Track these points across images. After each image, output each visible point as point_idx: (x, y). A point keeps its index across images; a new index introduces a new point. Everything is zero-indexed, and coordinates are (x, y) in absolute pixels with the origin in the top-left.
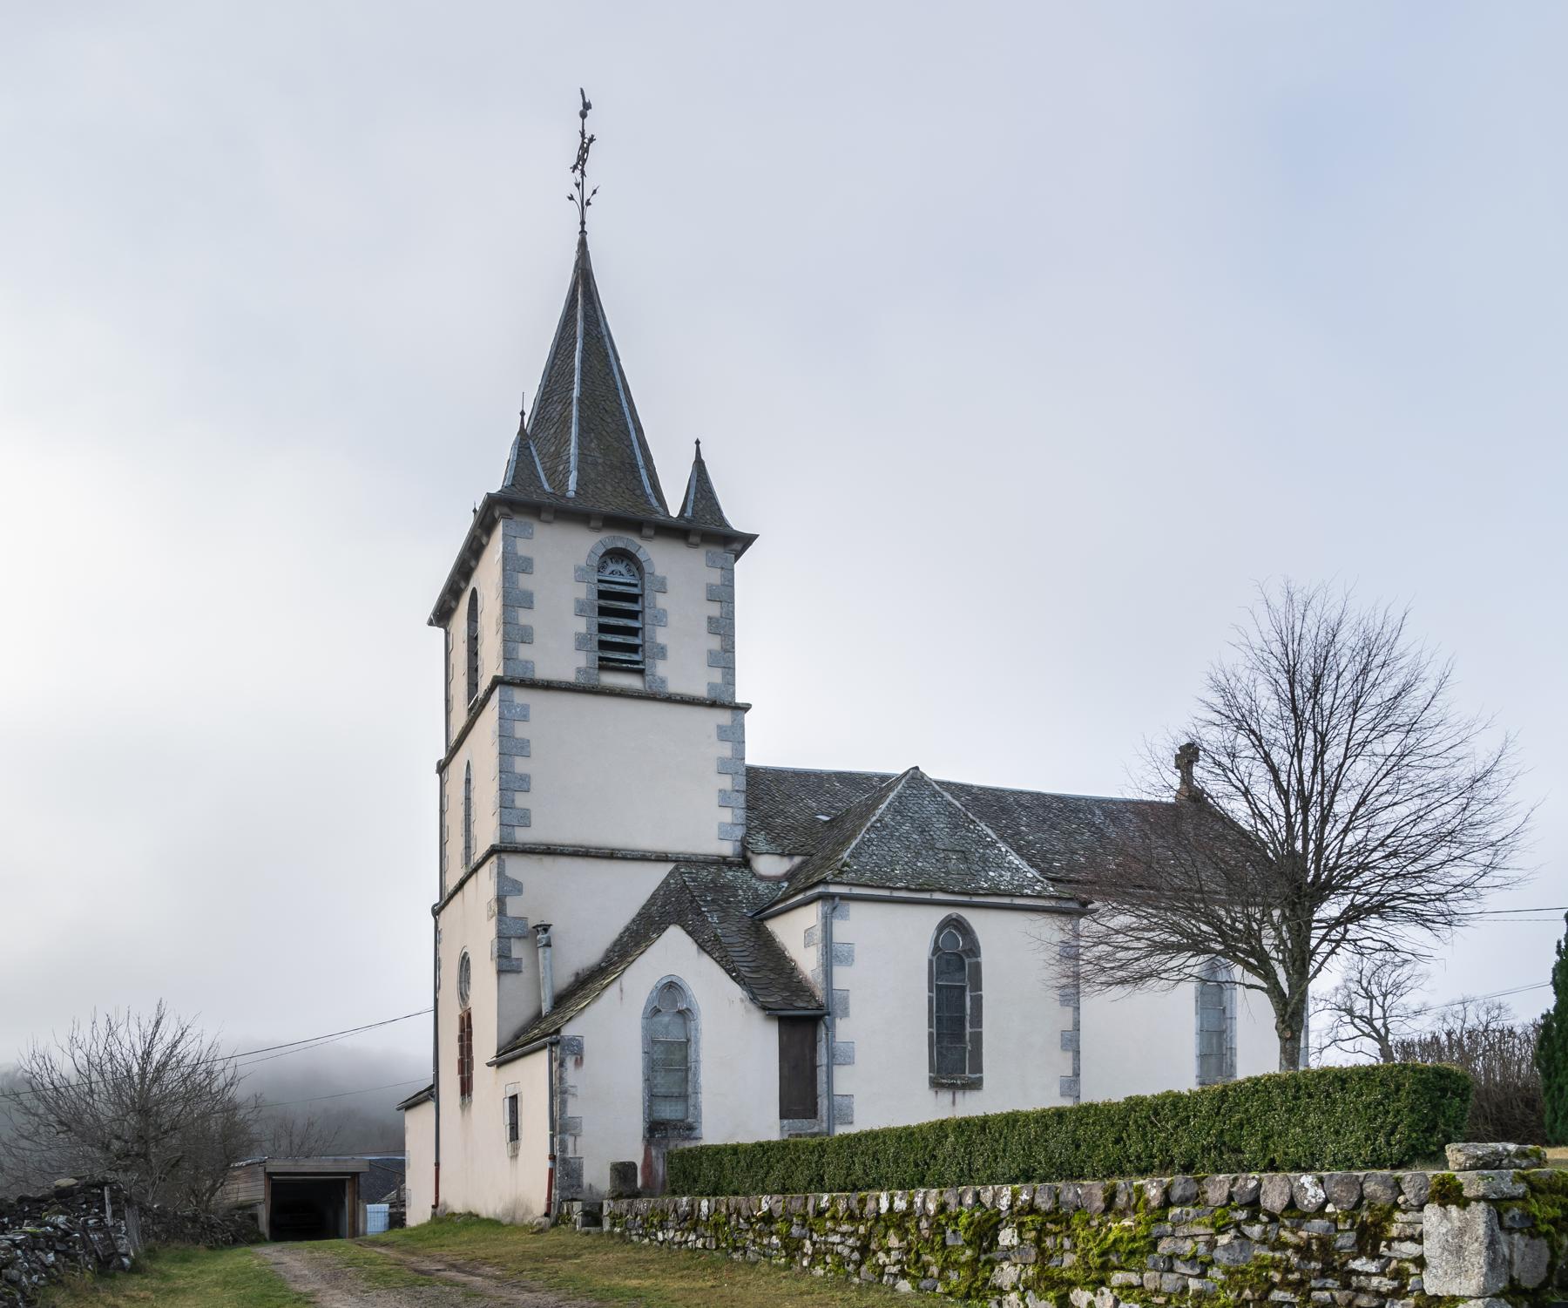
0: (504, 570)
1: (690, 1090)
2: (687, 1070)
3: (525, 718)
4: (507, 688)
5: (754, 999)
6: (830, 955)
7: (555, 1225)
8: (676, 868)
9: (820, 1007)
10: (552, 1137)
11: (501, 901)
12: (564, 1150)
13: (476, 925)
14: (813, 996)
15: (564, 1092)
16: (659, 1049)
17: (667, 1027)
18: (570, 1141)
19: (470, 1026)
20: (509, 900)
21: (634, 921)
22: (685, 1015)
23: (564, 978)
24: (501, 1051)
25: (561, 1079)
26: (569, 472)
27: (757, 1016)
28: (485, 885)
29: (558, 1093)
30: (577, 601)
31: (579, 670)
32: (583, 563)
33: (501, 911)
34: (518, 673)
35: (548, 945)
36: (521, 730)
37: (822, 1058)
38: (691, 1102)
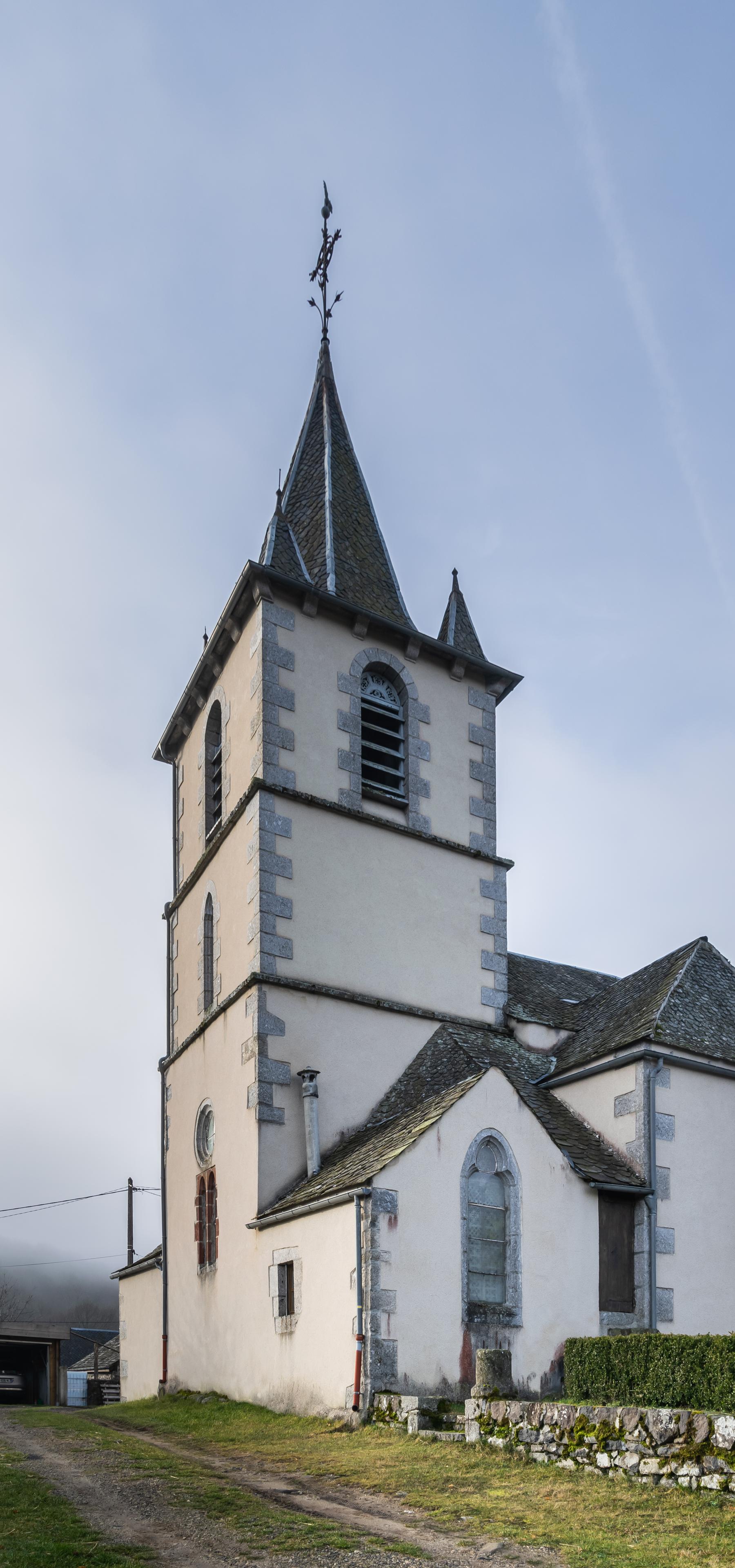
0: (264, 660)
1: (509, 1269)
2: (505, 1245)
3: (286, 834)
4: (268, 796)
5: (575, 1168)
6: (653, 1127)
7: (367, 1421)
8: (443, 1028)
9: (642, 1184)
10: (360, 1312)
11: (261, 1039)
12: (376, 1330)
13: (228, 1067)
14: (630, 1171)
15: (376, 1258)
16: (475, 1216)
17: (482, 1190)
18: (383, 1318)
19: (212, 1186)
20: (270, 1039)
21: (400, 1081)
22: (504, 1177)
23: (329, 1138)
24: (261, 1214)
25: (373, 1241)
26: (326, 575)
27: (578, 1188)
28: (242, 1021)
29: (369, 1258)
30: (340, 712)
31: (342, 792)
32: (346, 672)
33: (263, 1052)
34: (279, 781)
35: (315, 1095)
36: (283, 848)
37: (642, 1242)
38: (509, 1283)
